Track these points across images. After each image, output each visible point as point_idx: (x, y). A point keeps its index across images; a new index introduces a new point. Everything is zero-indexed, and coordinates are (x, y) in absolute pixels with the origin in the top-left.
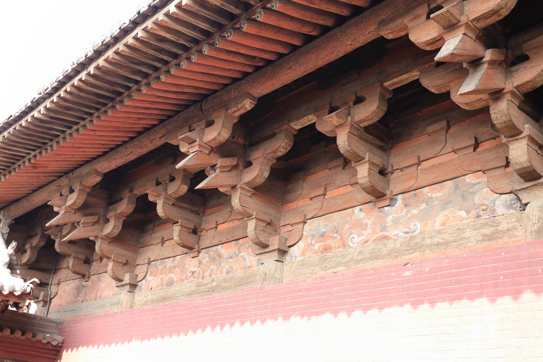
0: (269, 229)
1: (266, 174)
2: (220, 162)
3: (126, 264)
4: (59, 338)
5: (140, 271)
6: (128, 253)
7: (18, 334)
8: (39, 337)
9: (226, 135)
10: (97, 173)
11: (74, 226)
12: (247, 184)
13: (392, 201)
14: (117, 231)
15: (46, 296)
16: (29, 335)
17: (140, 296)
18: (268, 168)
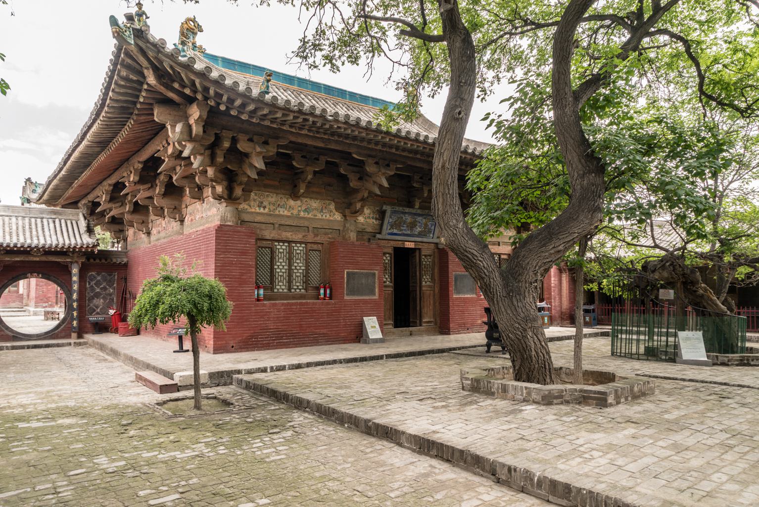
0: (175, 211)
1: (163, 190)
2: (142, 187)
3: (143, 222)
4: (125, 260)
5: (150, 226)
6: (143, 217)
7: (103, 261)
8: (114, 260)
9: (137, 178)
10: (110, 185)
11: (111, 210)
12: (158, 194)
13: (203, 201)
14: (132, 209)
15: (123, 237)
16: (109, 260)
17: (153, 238)
18: (164, 187)
